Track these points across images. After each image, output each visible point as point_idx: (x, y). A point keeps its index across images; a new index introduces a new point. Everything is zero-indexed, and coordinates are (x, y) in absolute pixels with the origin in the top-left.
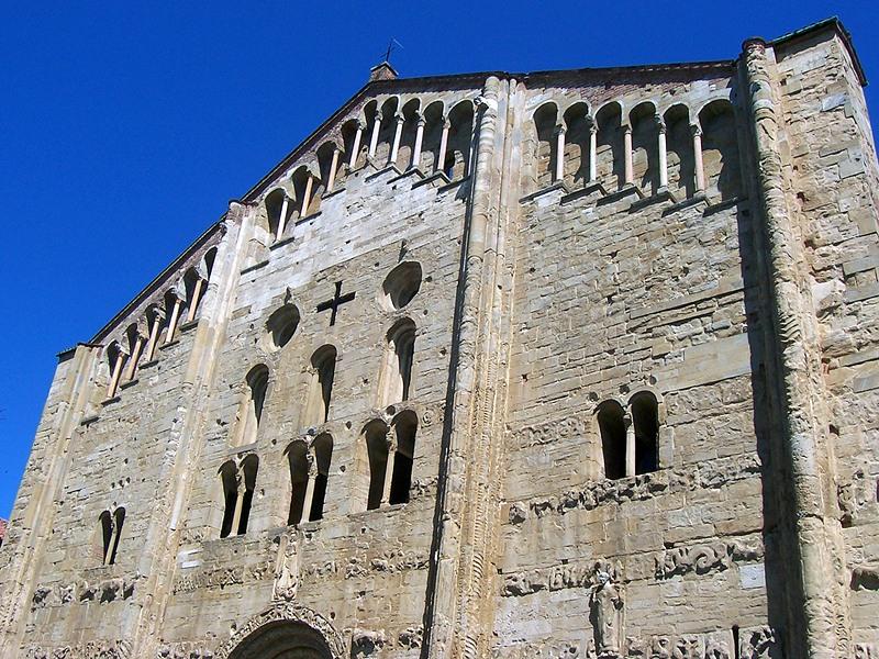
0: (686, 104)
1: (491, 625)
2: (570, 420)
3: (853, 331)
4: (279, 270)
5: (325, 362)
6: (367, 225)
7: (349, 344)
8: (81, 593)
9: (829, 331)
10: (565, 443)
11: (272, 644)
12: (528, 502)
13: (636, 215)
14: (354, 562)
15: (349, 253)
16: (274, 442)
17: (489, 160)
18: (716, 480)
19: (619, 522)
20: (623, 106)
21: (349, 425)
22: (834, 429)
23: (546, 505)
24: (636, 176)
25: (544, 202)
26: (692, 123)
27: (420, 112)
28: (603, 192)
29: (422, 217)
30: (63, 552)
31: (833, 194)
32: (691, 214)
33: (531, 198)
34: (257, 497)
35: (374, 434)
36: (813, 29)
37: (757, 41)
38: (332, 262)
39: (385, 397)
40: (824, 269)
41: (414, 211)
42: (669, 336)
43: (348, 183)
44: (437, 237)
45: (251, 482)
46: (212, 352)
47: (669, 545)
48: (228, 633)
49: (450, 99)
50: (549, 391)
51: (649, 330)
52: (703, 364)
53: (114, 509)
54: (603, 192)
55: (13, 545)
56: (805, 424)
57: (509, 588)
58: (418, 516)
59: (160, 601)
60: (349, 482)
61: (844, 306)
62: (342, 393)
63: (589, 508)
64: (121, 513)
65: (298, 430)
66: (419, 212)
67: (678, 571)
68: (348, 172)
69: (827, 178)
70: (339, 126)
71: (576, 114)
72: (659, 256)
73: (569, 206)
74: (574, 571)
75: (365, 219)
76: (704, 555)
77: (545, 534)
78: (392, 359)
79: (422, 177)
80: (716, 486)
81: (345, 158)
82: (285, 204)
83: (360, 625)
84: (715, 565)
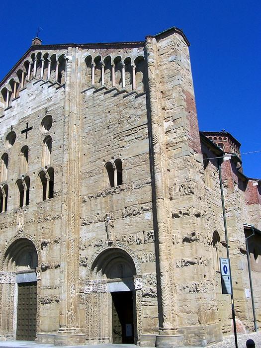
1: (79, 235)
2: (98, 169)
3: (175, 138)
4: (8, 119)
5: (25, 151)
6: (35, 101)
7: (32, 145)
9: (168, 139)
10: (96, 177)
11: (19, 246)
13: (115, 98)
14: (39, 218)
15: (30, 112)
16: (12, 180)
17: (70, 79)
18: (138, 187)
19: (112, 201)
21: (34, 173)
22: (168, 170)
23: (92, 196)
24: (116, 83)
25: (89, 93)
26: (132, 65)
27: (49, 58)
28: (106, 89)
31: (171, 91)
32: (131, 98)
33: (84, 92)
34: (9, 199)
35: (42, 175)
36: (161, 34)
37: (149, 36)
38: (27, 115)
39: (45, 162)
42: (125, 140)
43: (28, 85)
45: (7, 193)
47: (126, 208)
49: (58, 53)
50: (91, 159)
51: (119, 138)
52: (134, 150)
54: (106, 89)
56: (159, 170)
57: (83, 223)
58: (57, 202)
60: (36, 191)
61: (172, 130)
62: (31, 162)
63: (104, 197)
65: (19, 175)
67: (128, 215)
68: (27, 81)
69: (169, 86)
70: (23, 62)
71: (98, 59)
74: (101, 217)
77: (92, 206)
78: (46, 148)
79: (51, 83)
80: (138, 189)
81: (26, 74)
82: (8, 94)
84: (138, 213)
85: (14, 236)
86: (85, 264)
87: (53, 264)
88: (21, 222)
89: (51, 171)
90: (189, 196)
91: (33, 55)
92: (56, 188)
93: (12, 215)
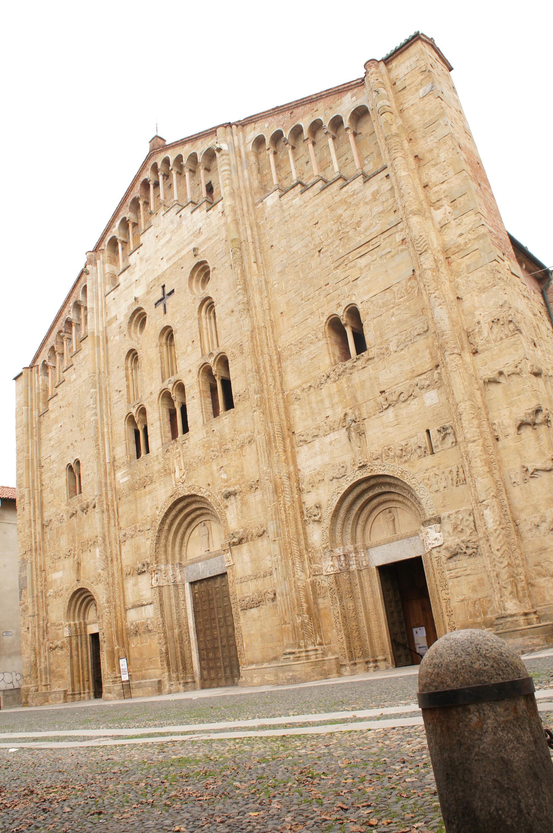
0: (340, 114)
3: (461, 235)
4: (127, 288)
8: (69, 515)
10: (313, 347)
12: (300, 388)
14: (213, 451)
15: (165, 266)
20: (303, 126)
29: (201, 231)
30: (52, 495)
31: (435, 151)
38: (156, 275)
40: (438, 201)
41: (195, 229)
44: (213, 241)
45: (144, 421)
46: (101, 350)
47: (382, 392)
48: (155, 513)
53: (72, 462)
55: (23, 500)
59: (113, 506)
64: (78, 462)
66: (199, 228)
68: (151, 213)
71: (277, 137)
72: (342, 218)
73: (285, 199)
75: (170, 239)
76: (402, 393)
77: (314, 405)
83: (225, 487)
85: (169, 494)
86: (317, 518)
87: (254, 531)
88: (178, 467)
89: (224, 361)
90: (513, 339)
91: (155, 166)
92: (236, 388)
93: (160, 457)
